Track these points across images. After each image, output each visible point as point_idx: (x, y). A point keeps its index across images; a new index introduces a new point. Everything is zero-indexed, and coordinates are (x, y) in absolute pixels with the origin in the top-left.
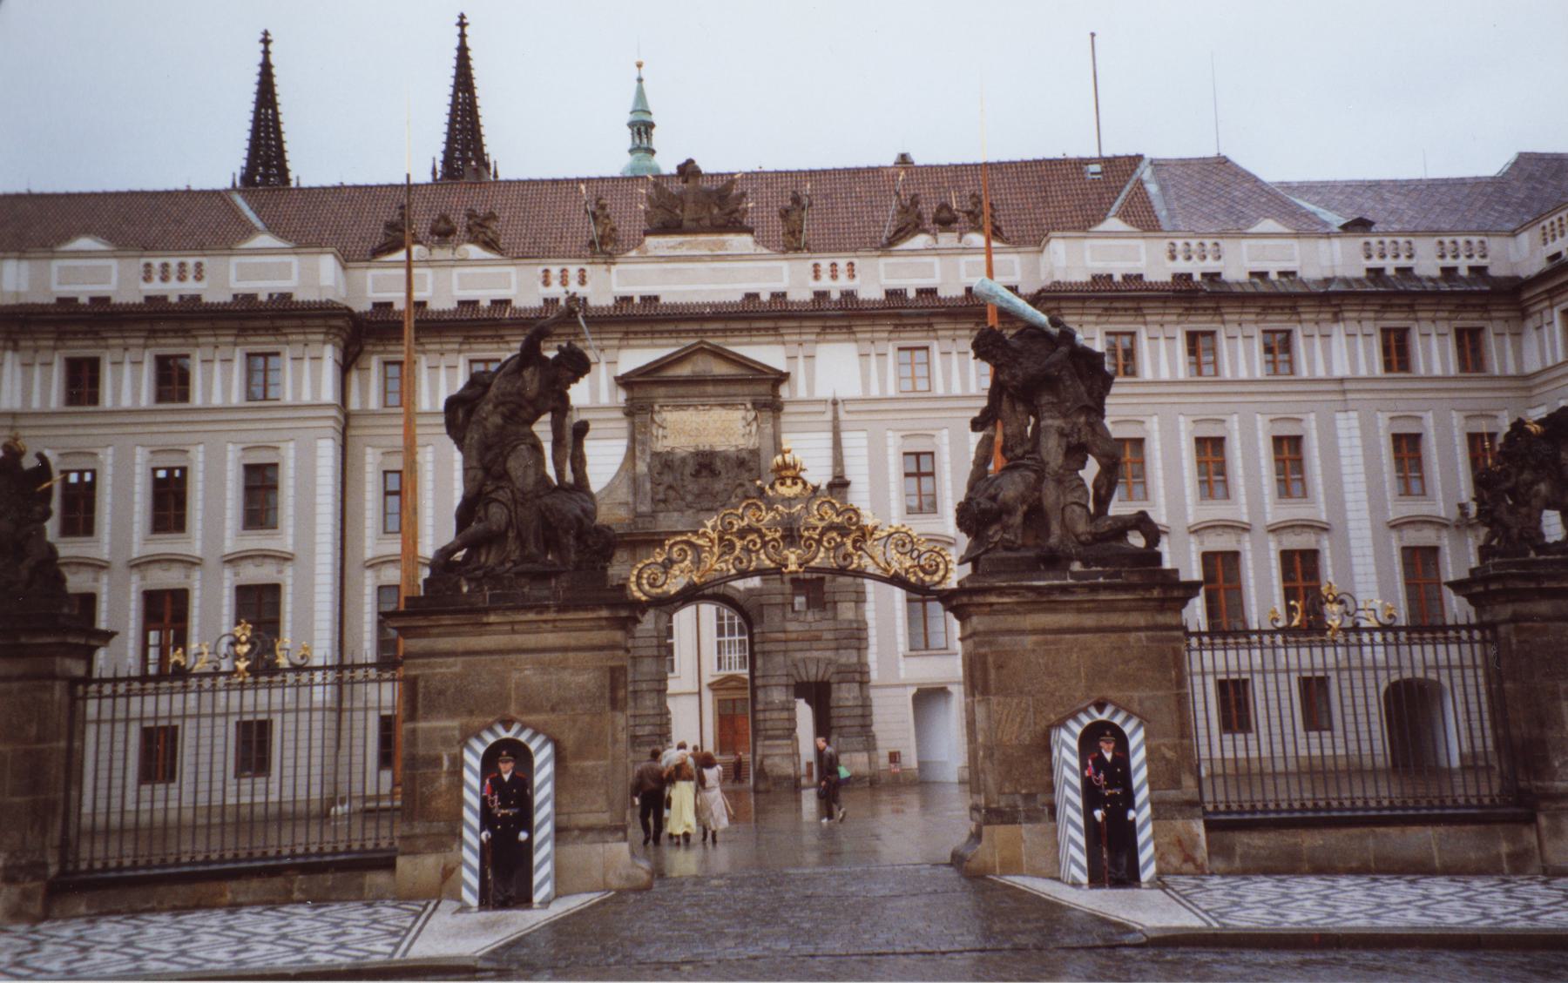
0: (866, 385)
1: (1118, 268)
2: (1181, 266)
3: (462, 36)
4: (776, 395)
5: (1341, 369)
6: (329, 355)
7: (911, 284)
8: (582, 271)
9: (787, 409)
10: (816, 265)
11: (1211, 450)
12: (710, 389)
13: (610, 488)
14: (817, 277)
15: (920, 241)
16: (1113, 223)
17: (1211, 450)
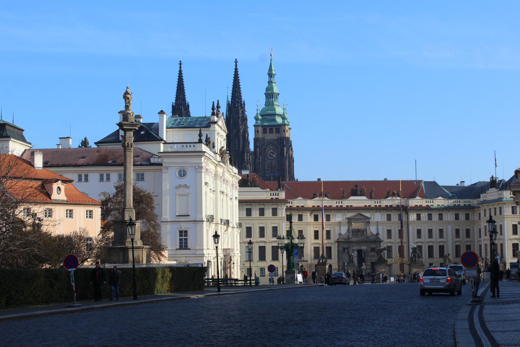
0: (382, 220)
1: (418, 204)
2: (427, 204)
3: (236, 65)
4: (369, 221)
5: (449, 219)
6: (309, 214)
7: (389, 204)
8: (342, 202)
9: (371, 223)
10: (375, 202)
11: (430, 231)
12: (360, 220)
13: (345, 234)
14: (375, 203)
15: (389, 198)
16: (418, 198)
17: (430, 231)
